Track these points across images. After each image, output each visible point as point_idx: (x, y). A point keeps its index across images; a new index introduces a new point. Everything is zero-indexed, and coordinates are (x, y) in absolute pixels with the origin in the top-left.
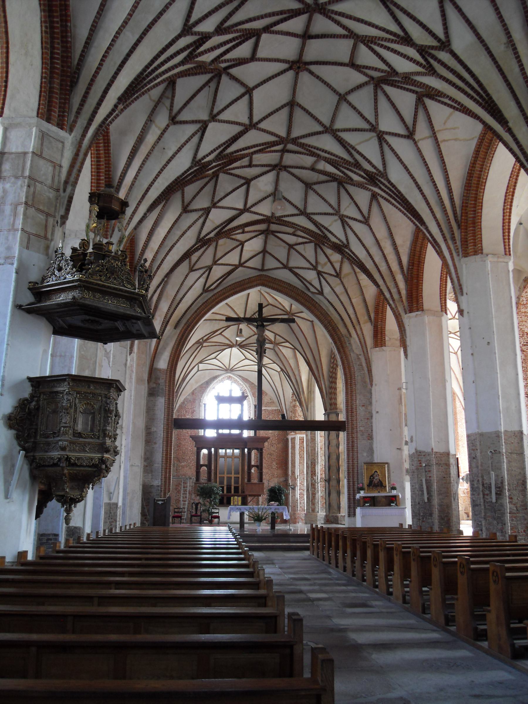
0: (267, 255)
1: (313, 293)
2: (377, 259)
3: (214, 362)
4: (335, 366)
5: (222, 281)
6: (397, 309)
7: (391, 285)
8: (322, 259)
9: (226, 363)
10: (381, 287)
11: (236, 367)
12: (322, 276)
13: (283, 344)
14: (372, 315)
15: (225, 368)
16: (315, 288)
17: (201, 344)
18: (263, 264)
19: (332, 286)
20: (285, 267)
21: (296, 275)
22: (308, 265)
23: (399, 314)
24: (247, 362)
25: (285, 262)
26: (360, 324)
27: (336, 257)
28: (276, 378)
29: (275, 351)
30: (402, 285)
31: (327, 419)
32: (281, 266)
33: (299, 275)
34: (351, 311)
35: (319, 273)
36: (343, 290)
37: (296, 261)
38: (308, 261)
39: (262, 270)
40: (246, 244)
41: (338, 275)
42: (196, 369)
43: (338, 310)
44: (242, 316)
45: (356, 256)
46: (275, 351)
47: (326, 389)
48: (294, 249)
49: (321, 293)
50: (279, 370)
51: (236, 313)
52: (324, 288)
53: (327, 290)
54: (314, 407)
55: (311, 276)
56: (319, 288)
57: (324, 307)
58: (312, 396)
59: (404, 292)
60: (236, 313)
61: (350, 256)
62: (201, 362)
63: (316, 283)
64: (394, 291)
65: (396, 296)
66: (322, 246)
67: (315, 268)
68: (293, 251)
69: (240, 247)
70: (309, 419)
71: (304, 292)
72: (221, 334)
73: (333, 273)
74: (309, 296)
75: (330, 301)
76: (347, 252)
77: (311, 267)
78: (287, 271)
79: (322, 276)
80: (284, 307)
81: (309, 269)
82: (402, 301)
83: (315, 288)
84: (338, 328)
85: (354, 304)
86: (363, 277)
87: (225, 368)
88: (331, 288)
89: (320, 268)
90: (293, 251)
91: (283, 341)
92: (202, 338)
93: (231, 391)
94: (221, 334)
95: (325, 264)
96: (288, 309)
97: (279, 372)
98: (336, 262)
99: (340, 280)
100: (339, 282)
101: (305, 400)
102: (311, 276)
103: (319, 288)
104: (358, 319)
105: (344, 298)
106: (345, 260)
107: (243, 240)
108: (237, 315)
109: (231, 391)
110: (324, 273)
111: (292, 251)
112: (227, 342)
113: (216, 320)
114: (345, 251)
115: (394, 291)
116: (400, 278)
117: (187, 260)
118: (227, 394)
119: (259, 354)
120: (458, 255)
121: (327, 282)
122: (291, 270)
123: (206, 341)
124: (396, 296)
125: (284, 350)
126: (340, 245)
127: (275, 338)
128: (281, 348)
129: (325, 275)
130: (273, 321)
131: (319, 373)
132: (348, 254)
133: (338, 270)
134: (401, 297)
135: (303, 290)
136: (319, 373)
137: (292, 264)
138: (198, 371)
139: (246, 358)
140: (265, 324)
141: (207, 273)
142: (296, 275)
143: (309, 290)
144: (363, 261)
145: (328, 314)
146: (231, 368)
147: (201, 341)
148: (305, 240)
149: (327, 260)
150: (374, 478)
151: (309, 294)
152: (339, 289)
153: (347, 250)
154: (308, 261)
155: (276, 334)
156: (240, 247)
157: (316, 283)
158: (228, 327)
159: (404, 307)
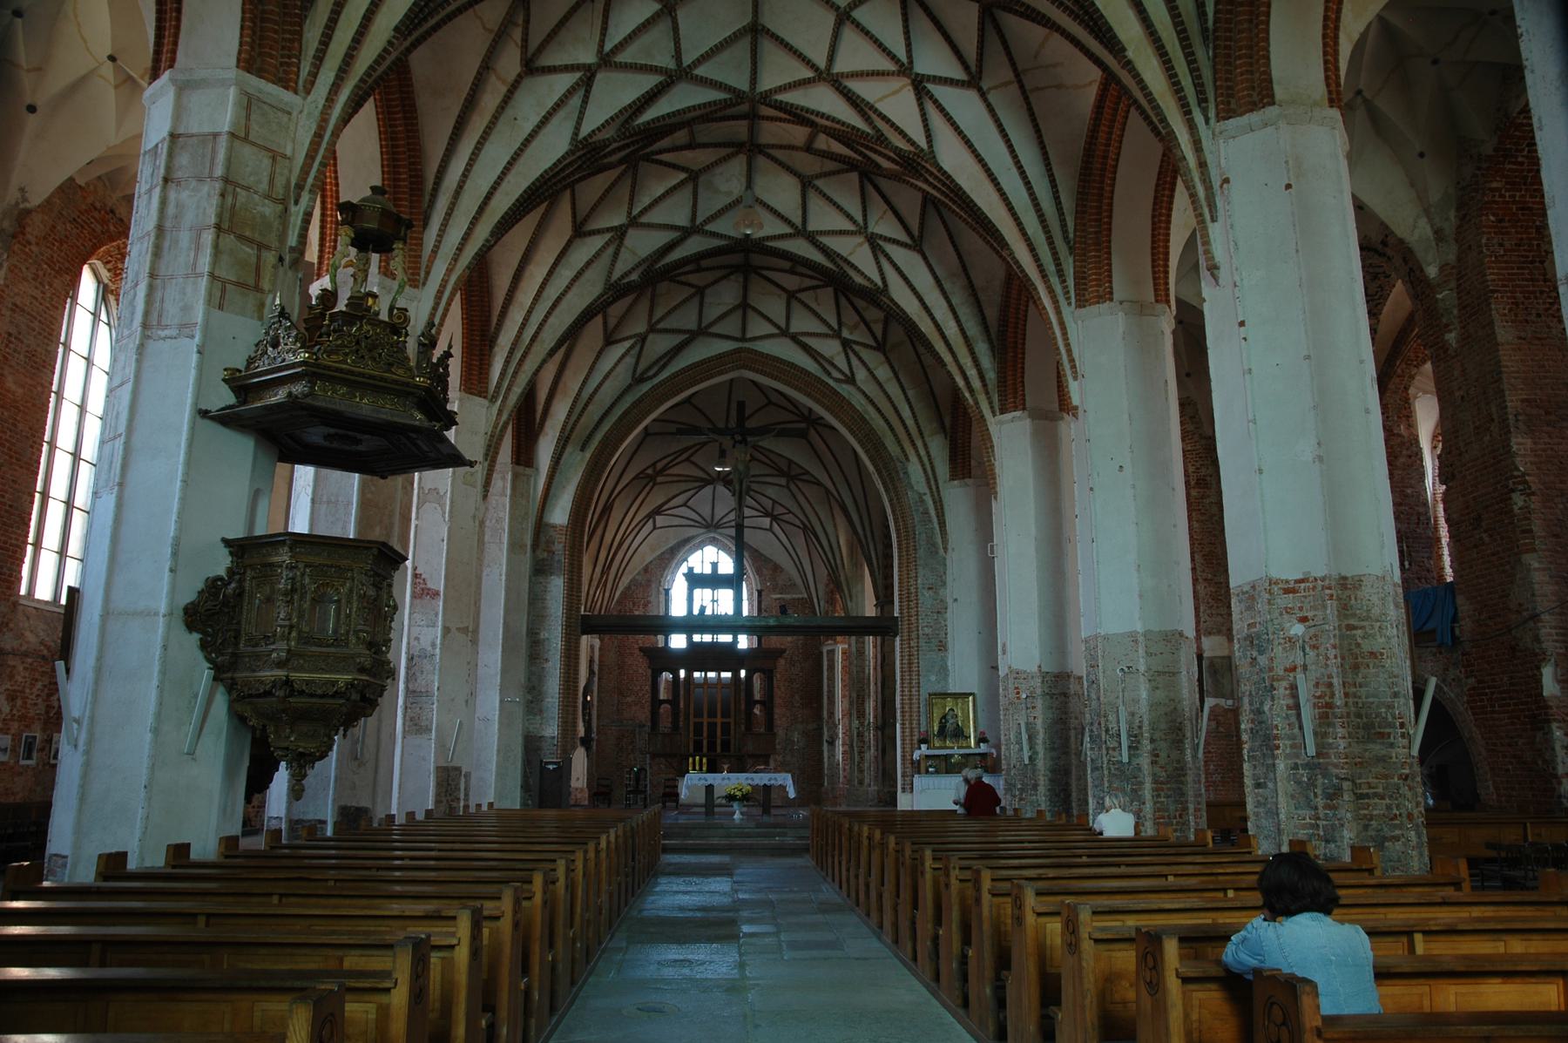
7: (967, 362)
8: (850, 316)
16: (840, 371)
19: (871, 366)
27: (873, 314)
30: (987, 362)
35: (846, 344)
49: (851, 380)
53: (861, 375)
55: (831, 348)
56: (847, 372)
63: (841, 361)
64: (972, 373)
65: (976, 384)
67: (837, 334)
78: (787, 342)
81: (826, 336)
89: (845, 334)
99: (885, 355)
100: (883, 359)
102: (831, 348)
103: (847, 372)
115: (972, 373)
116: (982, 348)
121: (860, 359)
124: (976, 384)
129: (857, 348)
135: (819, 375)
143: (829, 374)
152: (883, 372)
157: (841, 361)
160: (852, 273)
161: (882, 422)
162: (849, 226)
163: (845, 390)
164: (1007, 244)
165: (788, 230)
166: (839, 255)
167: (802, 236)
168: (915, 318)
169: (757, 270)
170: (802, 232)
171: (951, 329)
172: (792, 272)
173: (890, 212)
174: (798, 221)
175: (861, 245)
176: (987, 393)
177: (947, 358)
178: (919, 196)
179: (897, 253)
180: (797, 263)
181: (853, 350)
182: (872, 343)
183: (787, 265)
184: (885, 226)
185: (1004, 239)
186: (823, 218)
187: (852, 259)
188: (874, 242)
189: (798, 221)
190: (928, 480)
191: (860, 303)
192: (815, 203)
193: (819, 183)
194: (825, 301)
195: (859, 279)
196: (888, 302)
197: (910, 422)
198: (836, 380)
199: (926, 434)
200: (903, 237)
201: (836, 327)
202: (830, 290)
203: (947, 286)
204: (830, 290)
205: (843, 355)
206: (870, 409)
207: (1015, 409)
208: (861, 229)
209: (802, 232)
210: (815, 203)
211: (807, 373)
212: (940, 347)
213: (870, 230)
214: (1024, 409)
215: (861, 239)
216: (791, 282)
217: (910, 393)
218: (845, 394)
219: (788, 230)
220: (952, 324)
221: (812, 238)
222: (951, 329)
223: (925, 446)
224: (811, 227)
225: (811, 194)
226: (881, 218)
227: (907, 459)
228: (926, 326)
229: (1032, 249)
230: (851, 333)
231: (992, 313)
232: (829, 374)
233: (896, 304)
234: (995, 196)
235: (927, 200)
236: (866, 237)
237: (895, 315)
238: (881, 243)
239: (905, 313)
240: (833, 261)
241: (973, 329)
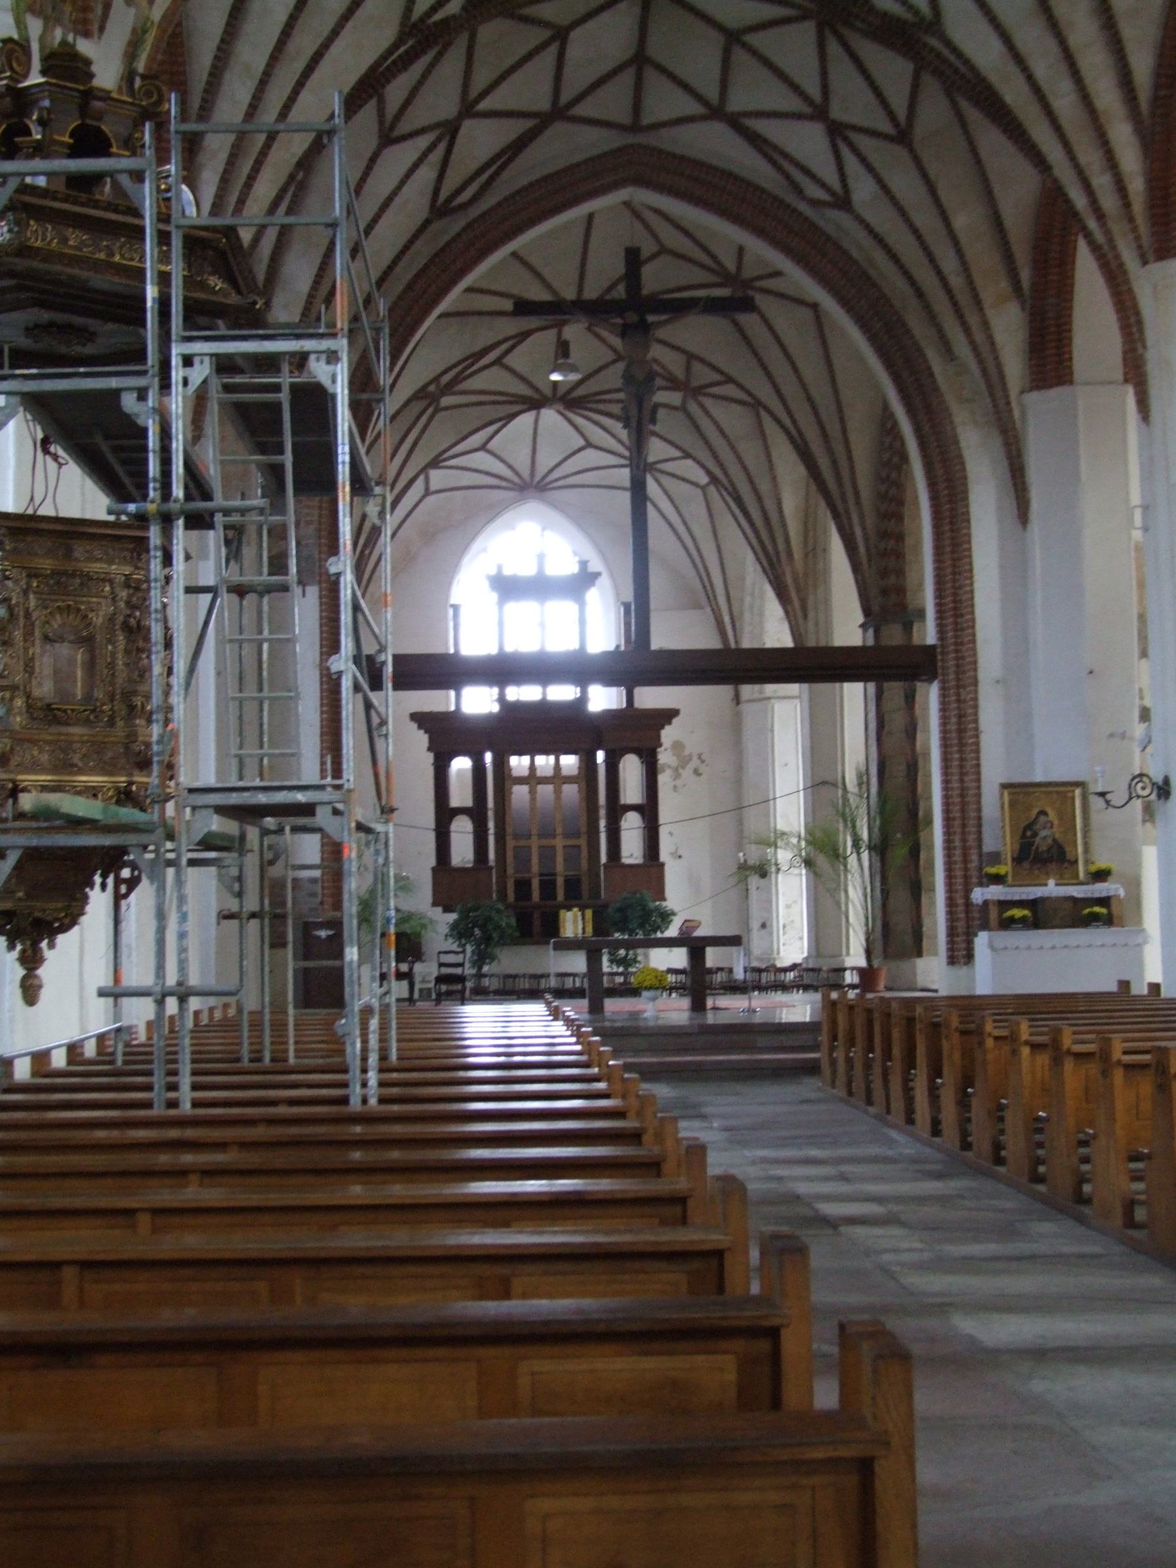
0: (650, 75)
1: (815, 203)
2: (1040, 70)
3: (481, 460)
4: (896, 460)
5: (497, 173)
6: (1113, 248)
7: (1090, 157)
9: (522, 461)
10: (1056, 172)
11: (557, 474)
12: (846, 139)
13: (715, 390)
14: (1025, 275)
15: (516, 479)
16: (823, 185)
17: (433, 399)
18: (637, 107)
20: (716, 112)
21: (755, 140)
22: (793, 103)
23: (1121, 265)
24: (591, 457)
25: (712, 93)
26: (981, 310)
28: (696, 509)
29: (689, 416)
30: (1130, 159)
31: (870, 642)
33: (765, 141)
34: (949, 264)
35: (837, 132)
38: (796, 88)
39: (635, 127)
40: (574, 35)
41: (903, 136)
42: (418, 487)
43: (904, 259)
44: (569, 294)
45: (967, 62)
46: (689, 416)
47: (866, 540)
48: (744, 45)
49: (843, 202)
50: (704, 479)
51: (548, 286)
52: (851, 182)
53: (863, 190)
54: (827, 601)
56: (836, 185)
57: (855, 253)
58: (821, 565)
59: (1137, 186)
60: (548, 286)
61: (945, 61)
62: (435, 463)
64: (1102, 181)
65: (1109, 202)
66: (845, 31)
67: (820, 112)
68: (740, 56)
69: (554, 49)
70: (811, 643)
71: (781, 201)
72: (498, 362)
73: (887, 127)
74: (800, 214)
75: (878, 229)
76: (932, 50)
77: (807, 110)
79: (846, 139)
80: (714, 257)
81: (799, 116)
82: (1131, 219)
83: (823, 185)
84: (904, 325)
85: (963, 239)
86: (991, 140)
87: (516, 479)
88: (880, 181)
90: (740, 56)
91: (717, 377)
92: (436, 379)
93: (541, 558)
94: (498, 362)
96: (731, 266)
97: (703, 488)
99: (911, 150)
101: (795, 580)
104: (974, 289)
105: (925, 219)
106: (927, 79)
107: (565, 21)
108: (554, 292)
109: (541, 558)
112: (522, 390)
113: (480, 313)
114: (925, 45)
115: (1102, 181)
116: (1123, 135)
117: (373, 103)
118: (527, 569)
119: (634, 424)
121: (863, 160)
122: (735, 122)
123: (448, 389)
124: (1109, 202)
125: (718, 410)
126: (905, 22)
127: (688, 369)
128: (708, 402)
130: (678, 308)
131: (840, 485)
132: (938, 55)
134: (1127, 205)
136: (840, 485)
137: (738, 102)
138: (427, 493)
139: (589, 445)
140: (651, 318)
141: (442, 147)
142: (755, 140)
143: (799, 191)
144: (993, 78)
145: (869, 278)
146: (537, 478)
147: (432, 388)
150: (1035, 835)
151: (803, 207)
153: (934, 42)
154: (796, 88)
155: (691, 357)
156: (554, 49)
158: (524, 335)
159: (1138, 238)
161: (901, 283)
202: (807, 30)
204: (807, 30)
206: (879, 256)
218: (830, 229)
241: (1107, 95)
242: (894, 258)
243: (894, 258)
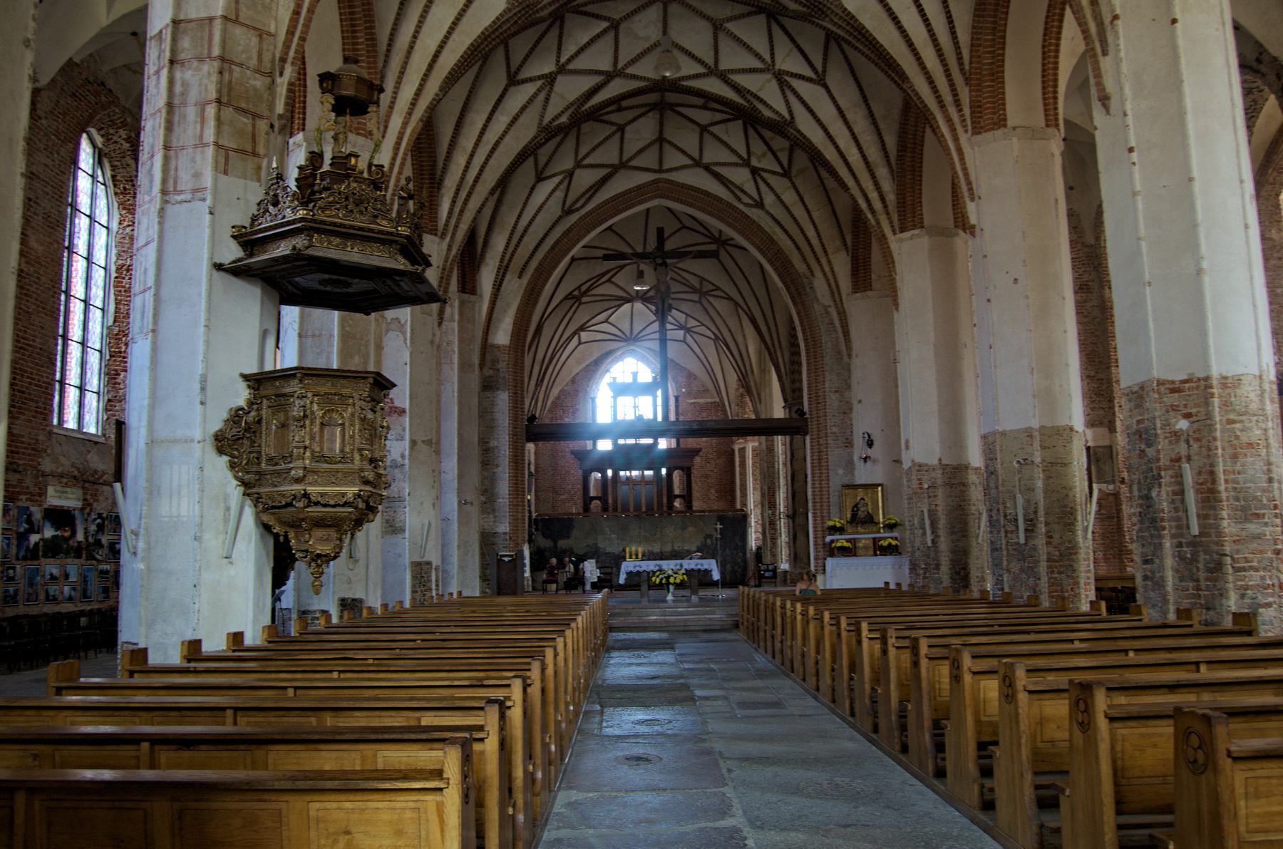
7: (868, 185)
8: (758, 148)
16: (751, 197)
19: (778, 191)
20: (698, 163)
27: (779, 143)
32: (690, 162)
35: (755, 172)
36: (797, 198)
37: (714, 154)
49: (760, 204)
53: (769, 199)
55: (741, 176)
56: (756, 196)
63: (750, 188)
64: (873, 196)
65: (878, 205)
67: (746, 163)
78: (700, 171)
81: (736, 165)
89: (754, 162)
95: (764, 155)
98: (782, 150)
99: (791, 180)
102: (741, 176)
103: (756, 196)
105: (799, 212)
110: (763, 170)
111: (706, 134)
115: (873, 196)
116: (882, 172)
120: (966, 131)
122: (707, 168)
124: (878, 205)
129: (765, 175)
133: (785, 163)
143: (740, 200)
148: (726, 116)
149: (765, 148)
152: (789, 197)
157: (750, 188)
160: (760, 107)
161: (789, 242)
162: (758, 65)
163: (754, 213)
164: (907, 78)
165: (701, 70)
166: (749, 91)
167: (716, 75)
168: (820, 147)
169: (672, 107)
170: (714, 71)
171: (854, 156)
172: (705, 107)
173: (795, 50)
174: (710, 62)
175: (769, 81)
176: (888, 214)
177: (850, 182)
178: (822, 34)
179: (802, 87)
180: (708, 100)
181: (763, 180)
182: (779, 169)
183: (700, 101)
184: (790, 62)
185: (904, 73)
186: (732, 59)
187: (761, 95)
188: (781, 79)
189: (710, 62)
190: (832, 293)
191: (768, 134)
192: (726, 45)
193: (729, 26)
194: (734, 134)
195: (767, 113)
196: (795, 133)
197: (815, 241)
198: (746, 205)
199: (829, 251)
200: (808, 73)
201: (745, 156)
202: (740, 122)
203: (849, 116)
204: (740, 122)
205: (752, 182)
206: (778, 230)
207: (914, 227)
208: (769, 68)
209: (714, 71)
210: (726, 45)
211: (720, 200)
212: (843, 172)
213: (777, 67)
214: (922, 227)
215: (768, 76)
216: (704, 117)
217: (815, 215)
218: (755, 218)
219: (701, 70)
220: (855, 151)
221: (723, 77)
222: (854, 156)
223: (829, 262)
224: (723, 66)
225: (721, 36)
226: (788, 55)
227: (813, 275)
228: (830, 154)
229: (931, 81)
230: (759, 162)
231: (891, 141)
232: (740, 200)
233: (802, 134)
234: (895, 33)
235: (830, 37)
236: (774, 74)
237: (800, 144)
238: (787, 78)
239: (810, 142)
240: (743, 97)
241: (874, 154)
242: (786, 231)
243: (786, 231)
